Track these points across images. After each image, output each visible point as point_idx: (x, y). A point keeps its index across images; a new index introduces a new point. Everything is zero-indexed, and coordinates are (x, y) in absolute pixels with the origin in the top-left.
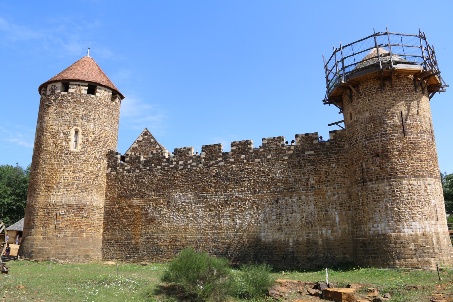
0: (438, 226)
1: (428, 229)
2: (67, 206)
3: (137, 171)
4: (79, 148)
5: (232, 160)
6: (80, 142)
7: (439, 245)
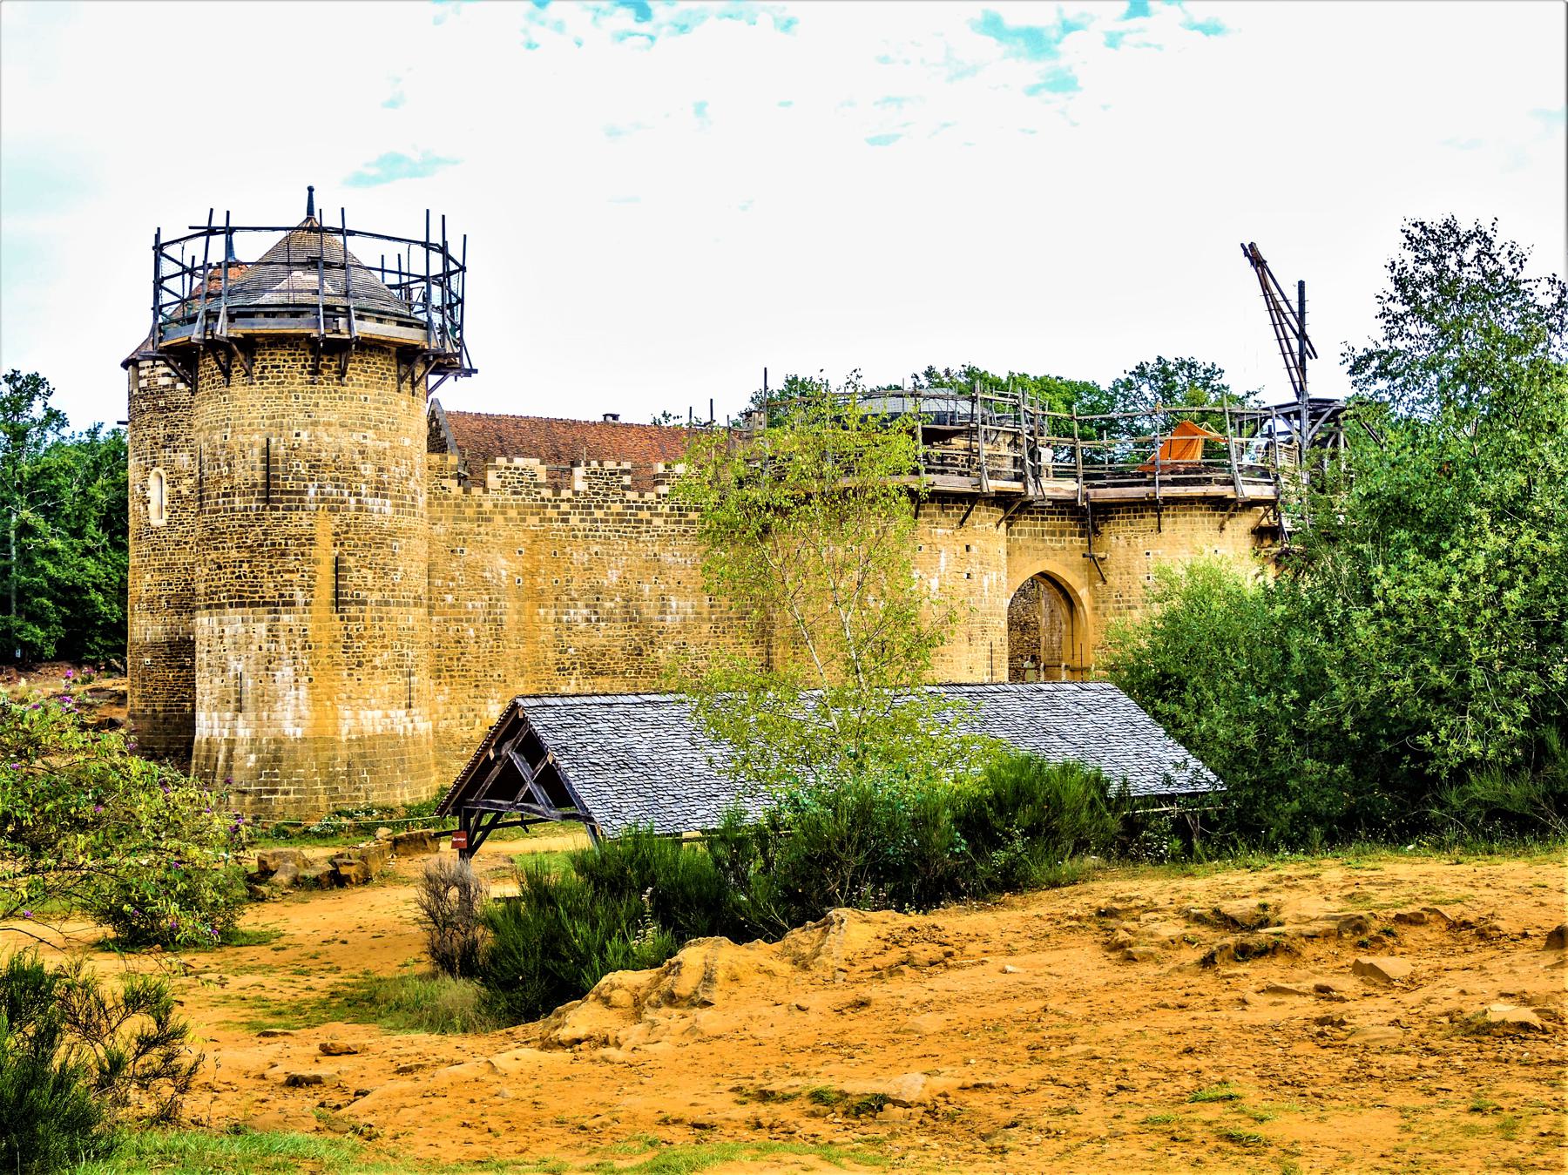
0: (241, 722)
1: (216, 732)
2: (154, 645)
4: (166, 515)
6: (166, 502)
7: (229, 768)
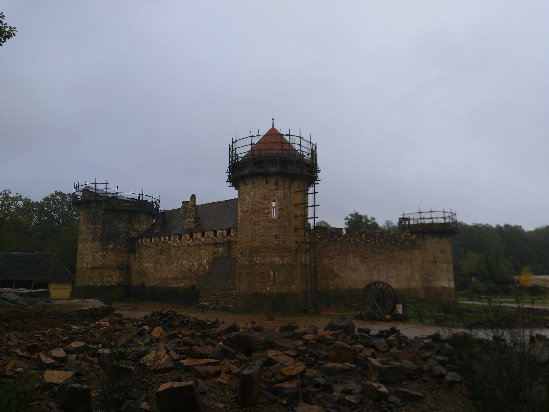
3: (326, 240)
5: (377, 241)
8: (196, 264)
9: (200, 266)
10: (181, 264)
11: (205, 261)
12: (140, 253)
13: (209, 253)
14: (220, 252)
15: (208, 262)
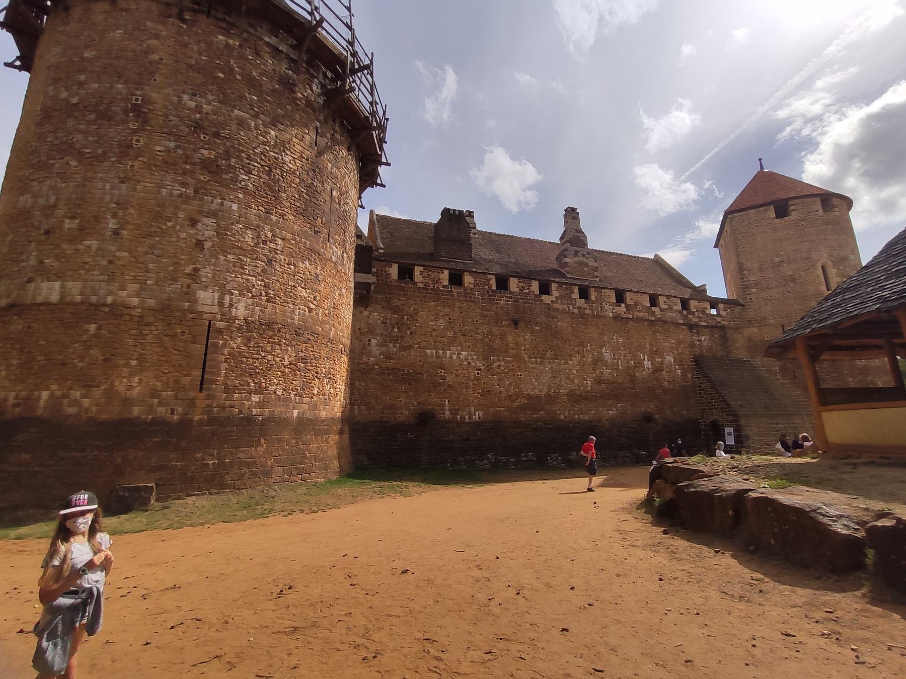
8: (647, 364)
9: (658, 369)
10: (598, 361)
11: (670, 358)
12: (395, 310)
13: (679, 342)
14: (705, 344)
15: (679, 361)
